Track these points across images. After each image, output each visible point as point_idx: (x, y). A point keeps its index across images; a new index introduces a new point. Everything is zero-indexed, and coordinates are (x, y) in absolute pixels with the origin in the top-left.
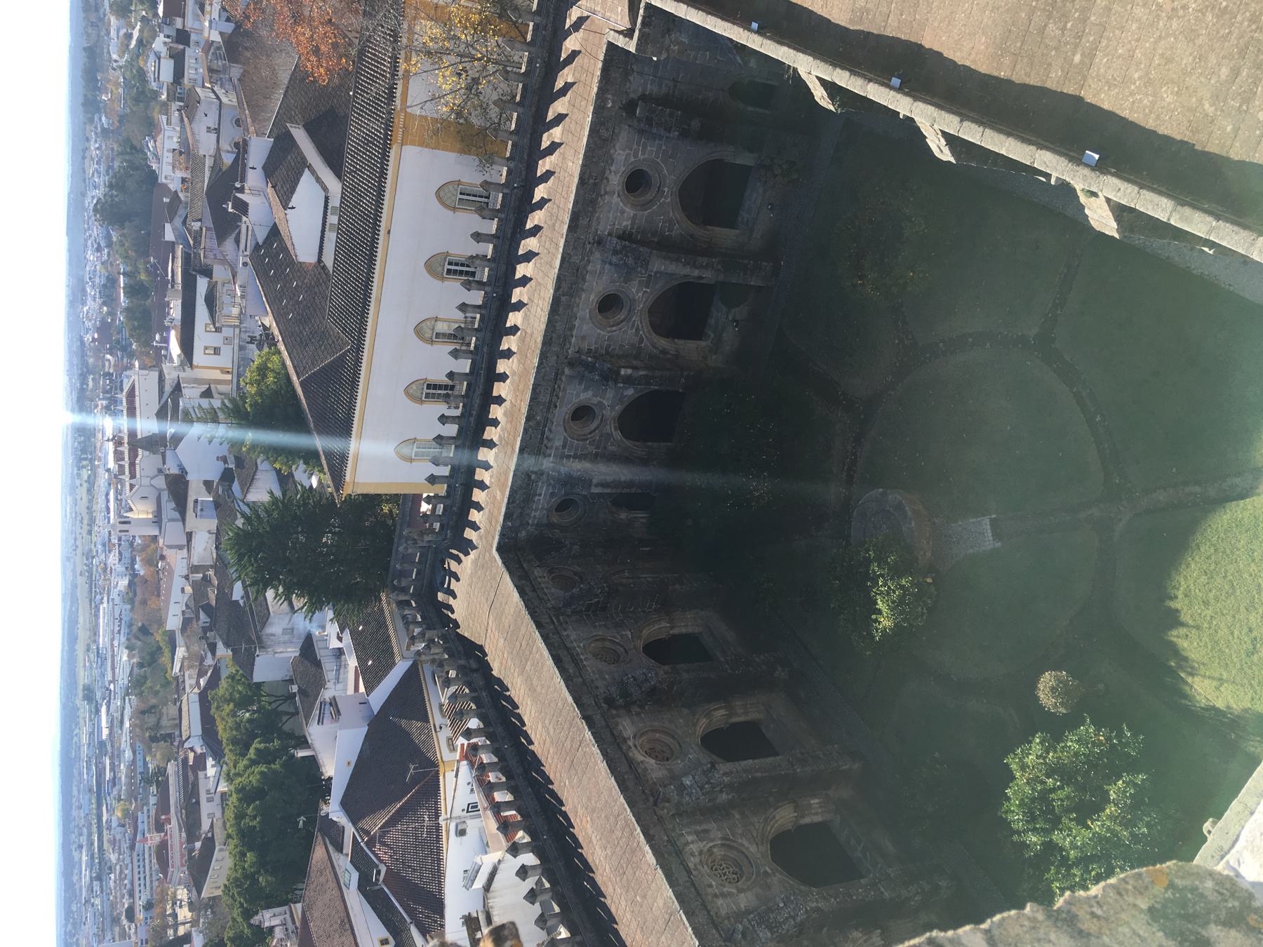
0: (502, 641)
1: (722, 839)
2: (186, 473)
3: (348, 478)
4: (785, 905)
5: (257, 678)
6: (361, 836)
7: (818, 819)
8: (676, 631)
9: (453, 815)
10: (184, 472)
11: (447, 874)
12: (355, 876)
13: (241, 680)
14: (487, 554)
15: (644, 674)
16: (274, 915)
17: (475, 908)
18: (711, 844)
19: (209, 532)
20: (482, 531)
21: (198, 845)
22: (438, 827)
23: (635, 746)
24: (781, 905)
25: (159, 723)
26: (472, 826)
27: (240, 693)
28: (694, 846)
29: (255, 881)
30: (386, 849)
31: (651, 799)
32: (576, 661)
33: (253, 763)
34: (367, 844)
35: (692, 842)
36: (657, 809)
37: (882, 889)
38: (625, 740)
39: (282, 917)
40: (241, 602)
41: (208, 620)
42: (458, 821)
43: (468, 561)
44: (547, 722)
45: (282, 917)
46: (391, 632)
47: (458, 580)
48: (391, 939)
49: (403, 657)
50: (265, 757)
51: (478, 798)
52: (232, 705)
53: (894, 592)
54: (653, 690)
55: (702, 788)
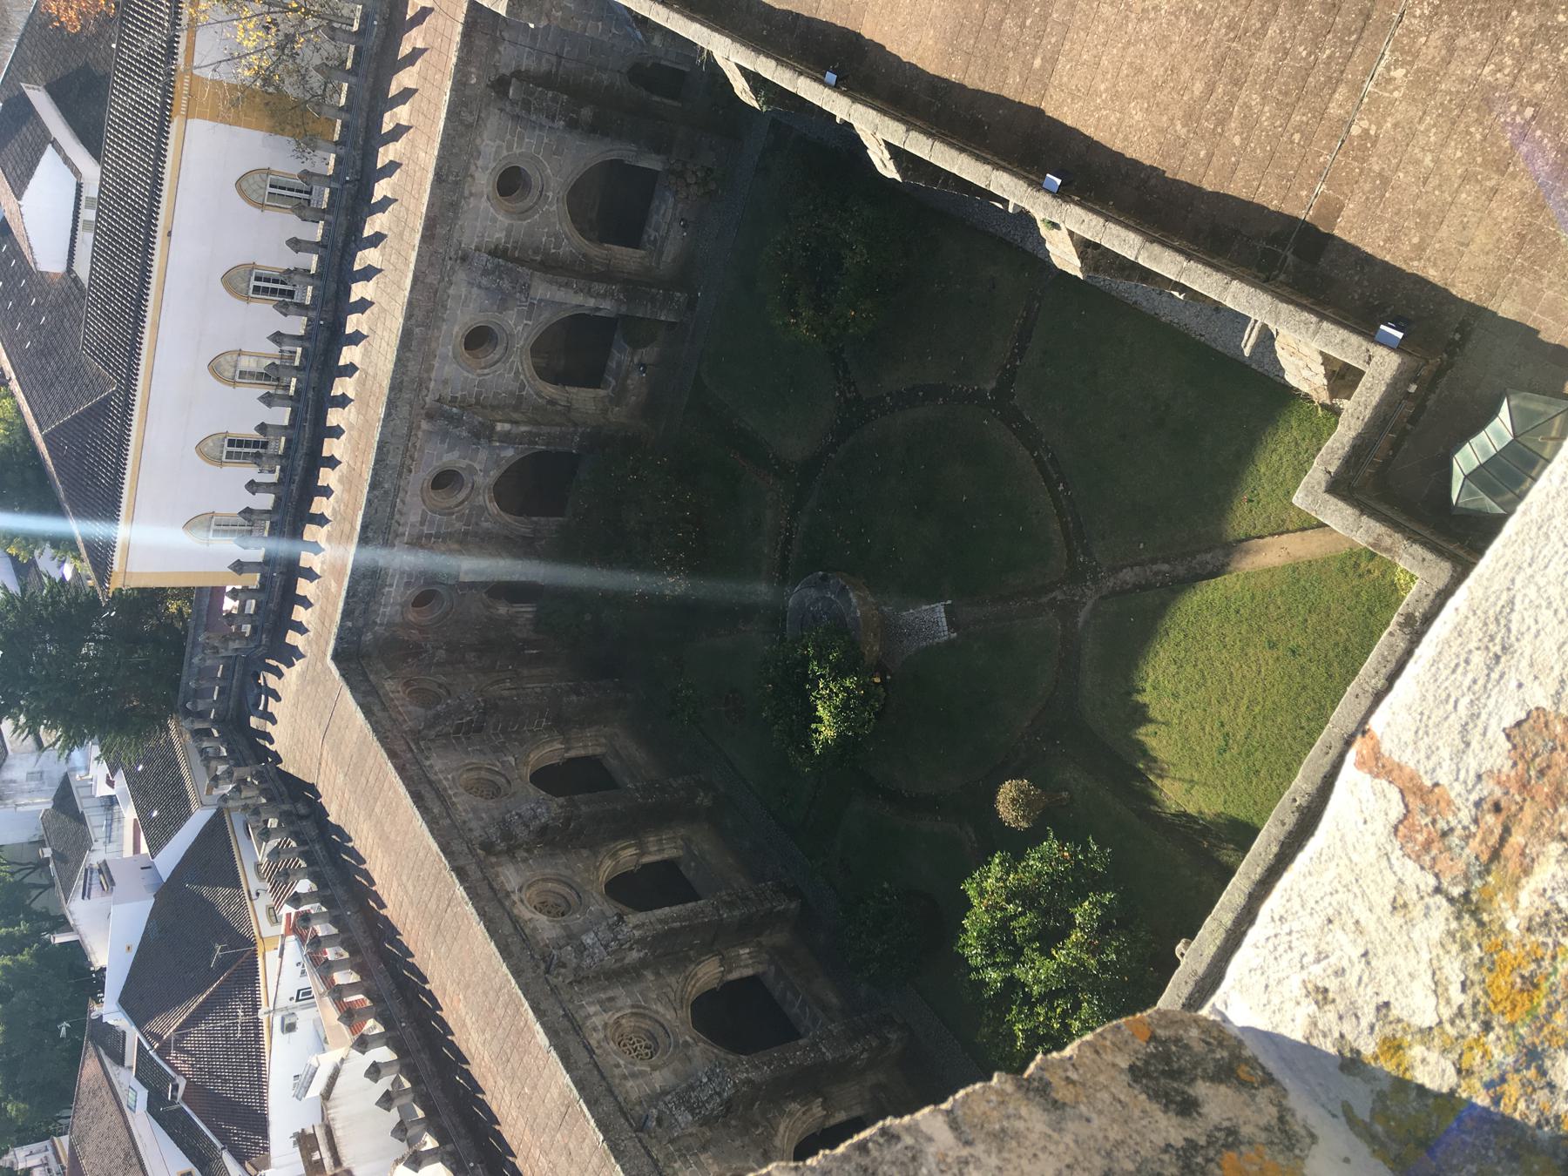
0: (341, 776)
1: (633, 1006)
3: (116, 567)
4: (709, 1080)
6: (149, 1043)
7: (749, 972)
8: (572, 754)
9: (278, 1007)
11: (271, 1083)
12: (143, 1094)
17: (308, 1121)
18: (619, 1015)
20: (311, 634)
22: (257, 1024)
23: (522, 901)
24: (705, 1080)
26: (304, 1018)
28: (596, 1018)
31: (543, 966)
32: (441, 796)
34: (158, 1051)
35: (595, 1014)
37: (824, 1050)
38: (508, 895)
42: (285, 1013)
43: (292, 674)
44: (404, 878)
46: (184, 771)
47: (278, 699)
51: (311, 981)
53: (837, 696)
54: (543, 831)
55: (606, 947)
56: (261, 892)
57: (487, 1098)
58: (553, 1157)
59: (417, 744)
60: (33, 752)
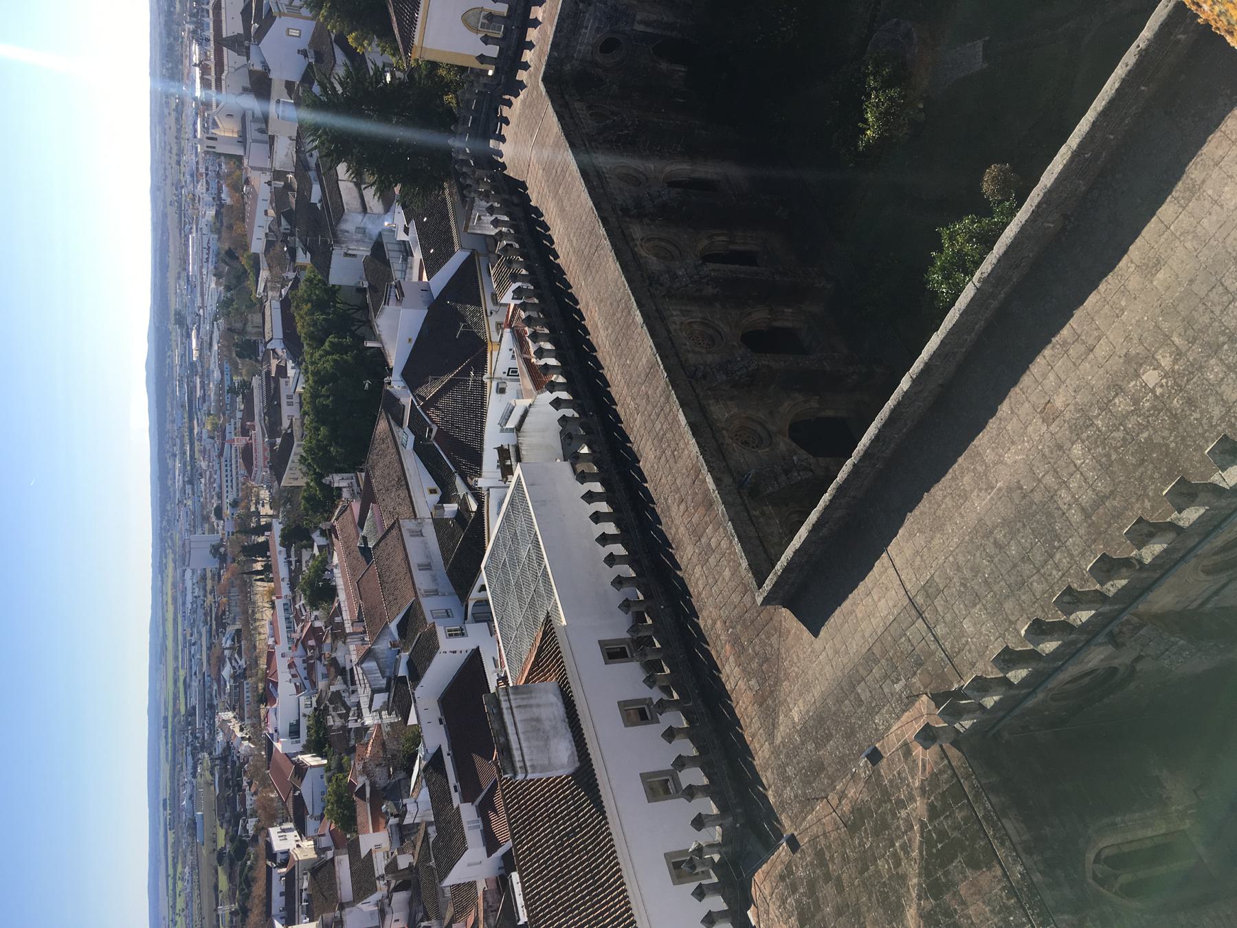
0: (541, 171)
2: (269, 70)
3: (416, 41)
4: (742, 359)
5: (334, 279)
7: (789, 325)
10: (267, 69)
11: (487, 423)
12: (412, 438)
13: (318, 284)
14: (535, 92)
15: (659, 191)
16: (343, 479)
17: (507, 440)
18: (691, 320)
19: (290, 138)
20: (531, 69)
21: (279, 440)
22: (483, 385)
23: (642, 246)
24: (739, 359)
25: (244, 328)
26: (511, 387)
27: (317, 295)
29: (325, 449)
30: (438, 413)
33: (327, 353)
36: (651, 289)
38: (633, 240)
39: (350, 481)
40: (319, 205)
41: (289, 227)
42: (500, 381)
43: (517, 102)
44: (572, 235)
45: (350, 481)
46: (452, 223)
47: (508, 123)
48: (439, 490)
49: (462, 248)
50: (336, 348)
51: (518, 364)
52: (309, 305)
53: (883, 105)
55: (691, 278)
56: (494, 313)
57: (605, 372)
58: (637, 401)
59: (590, 144)
60: (360, 213)
